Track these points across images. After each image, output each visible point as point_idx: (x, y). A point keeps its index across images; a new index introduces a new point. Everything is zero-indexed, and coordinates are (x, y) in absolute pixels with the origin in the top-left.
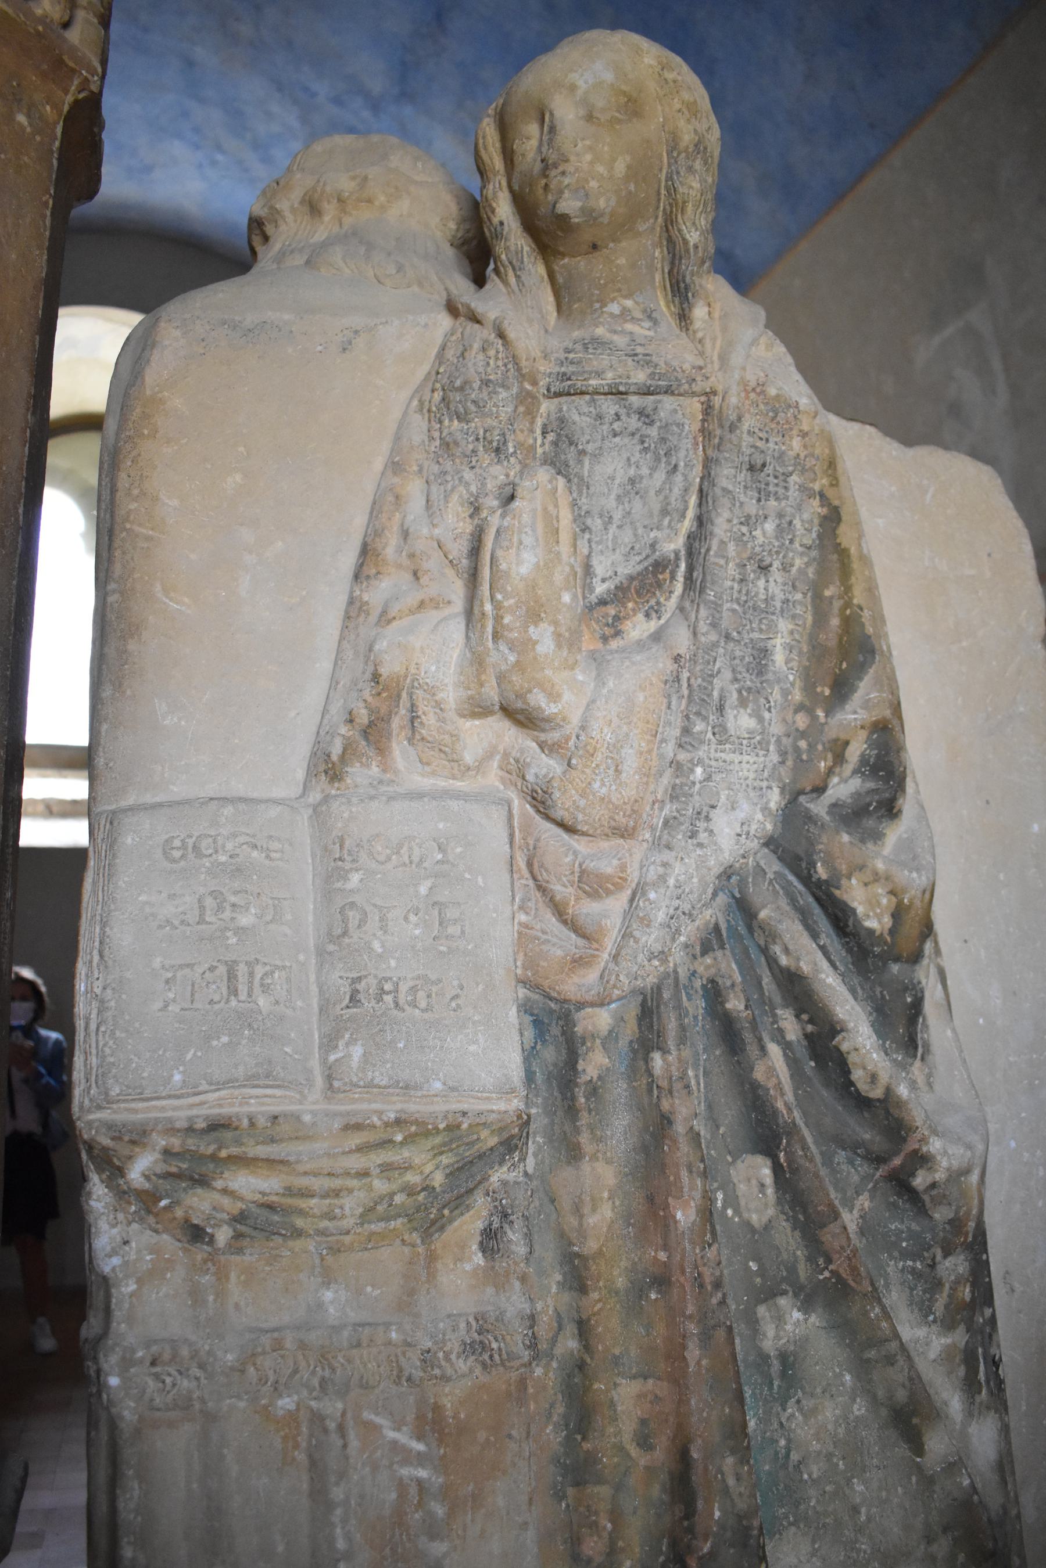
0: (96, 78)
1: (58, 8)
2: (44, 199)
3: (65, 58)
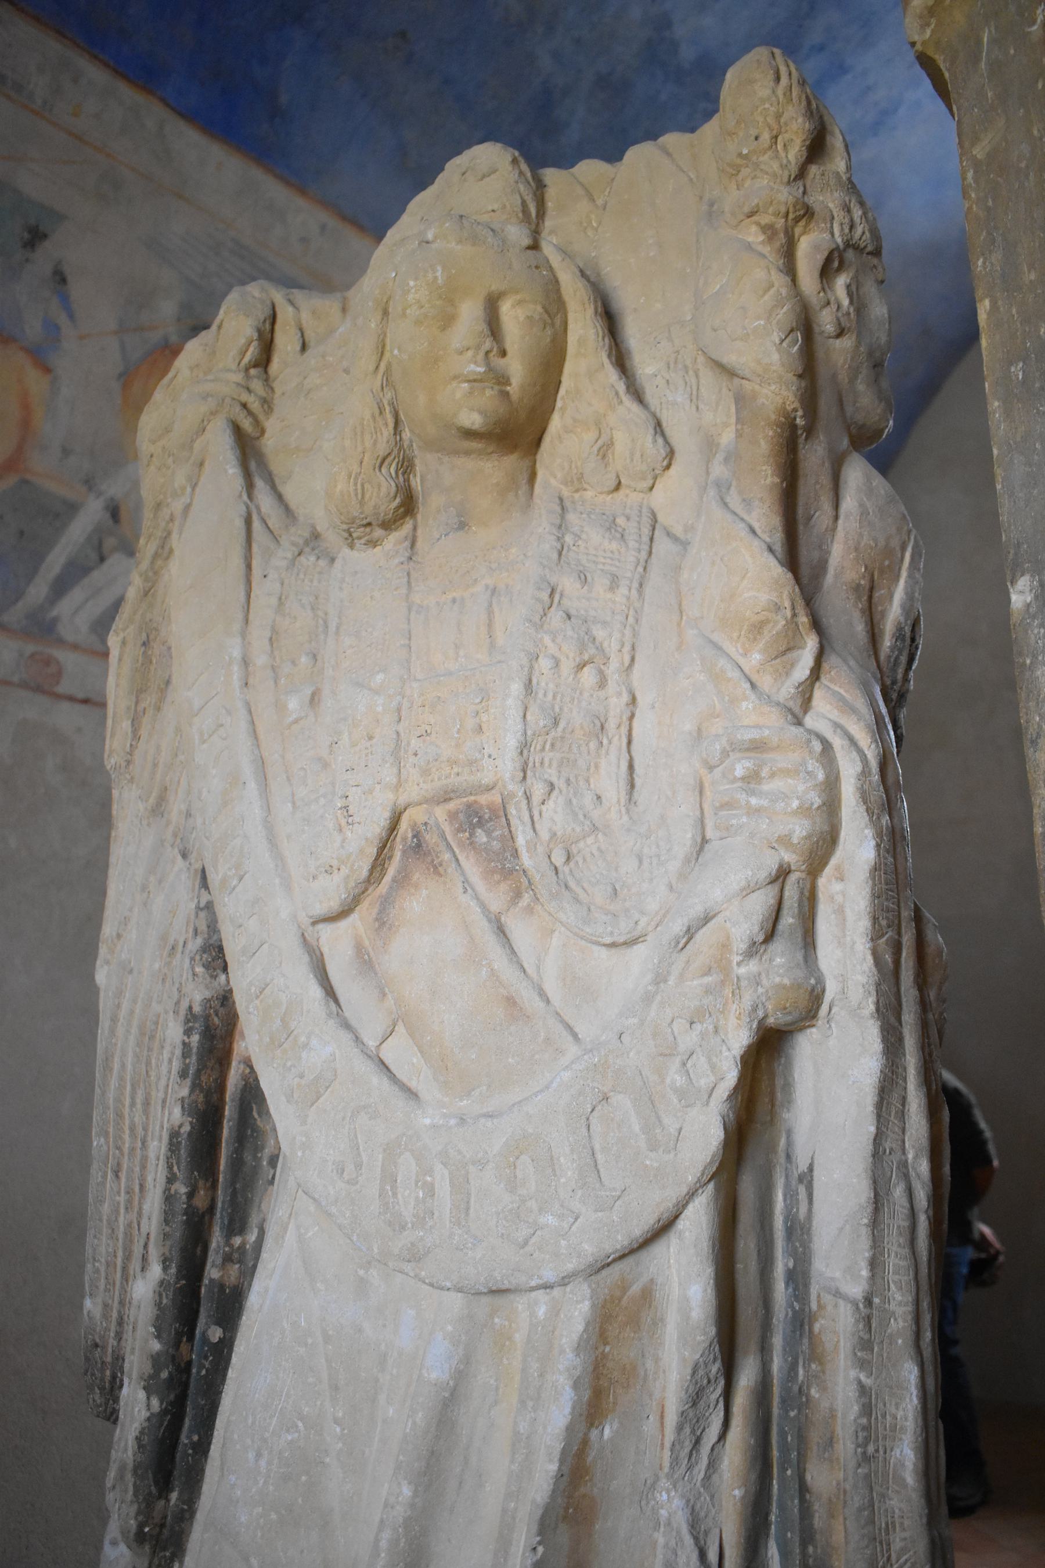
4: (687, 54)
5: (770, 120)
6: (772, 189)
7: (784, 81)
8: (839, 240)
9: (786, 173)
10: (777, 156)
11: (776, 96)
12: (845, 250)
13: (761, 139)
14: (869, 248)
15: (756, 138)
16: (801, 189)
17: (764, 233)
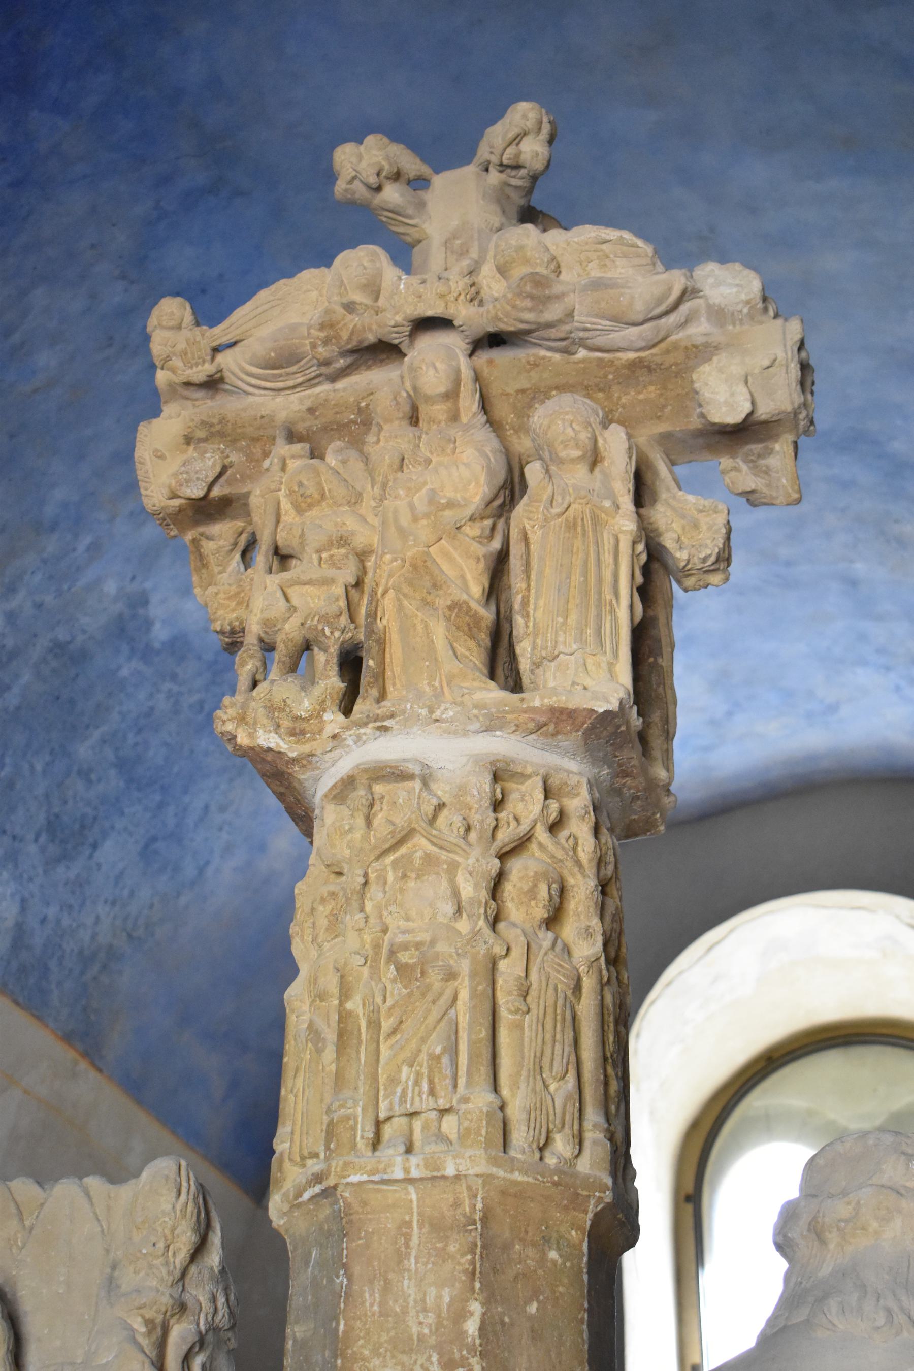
0: (608, 1193)
1: (568, 1148)
2: (580, 1317)
3: (580, 1191)
4: (160, 633)
5: (167, 1232)
6: (158, 1291)
7: (183, 1197)
8: (202, 1327)
9: (171, 1278)
10: (167, 1264)
11: (175, 1212)
12: (207, 1332)
13: (157, 1246)
14: (226, 1328)
15: (154, 1245)
16: (180, 1290)
17: (146, 1326)
